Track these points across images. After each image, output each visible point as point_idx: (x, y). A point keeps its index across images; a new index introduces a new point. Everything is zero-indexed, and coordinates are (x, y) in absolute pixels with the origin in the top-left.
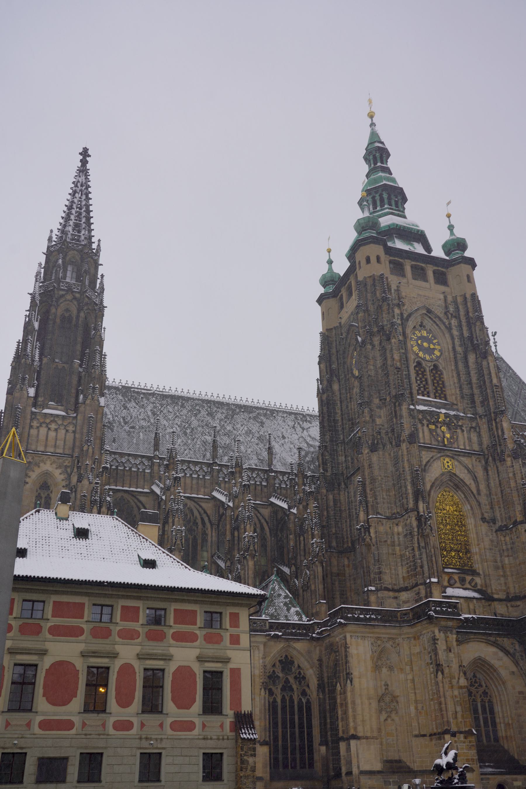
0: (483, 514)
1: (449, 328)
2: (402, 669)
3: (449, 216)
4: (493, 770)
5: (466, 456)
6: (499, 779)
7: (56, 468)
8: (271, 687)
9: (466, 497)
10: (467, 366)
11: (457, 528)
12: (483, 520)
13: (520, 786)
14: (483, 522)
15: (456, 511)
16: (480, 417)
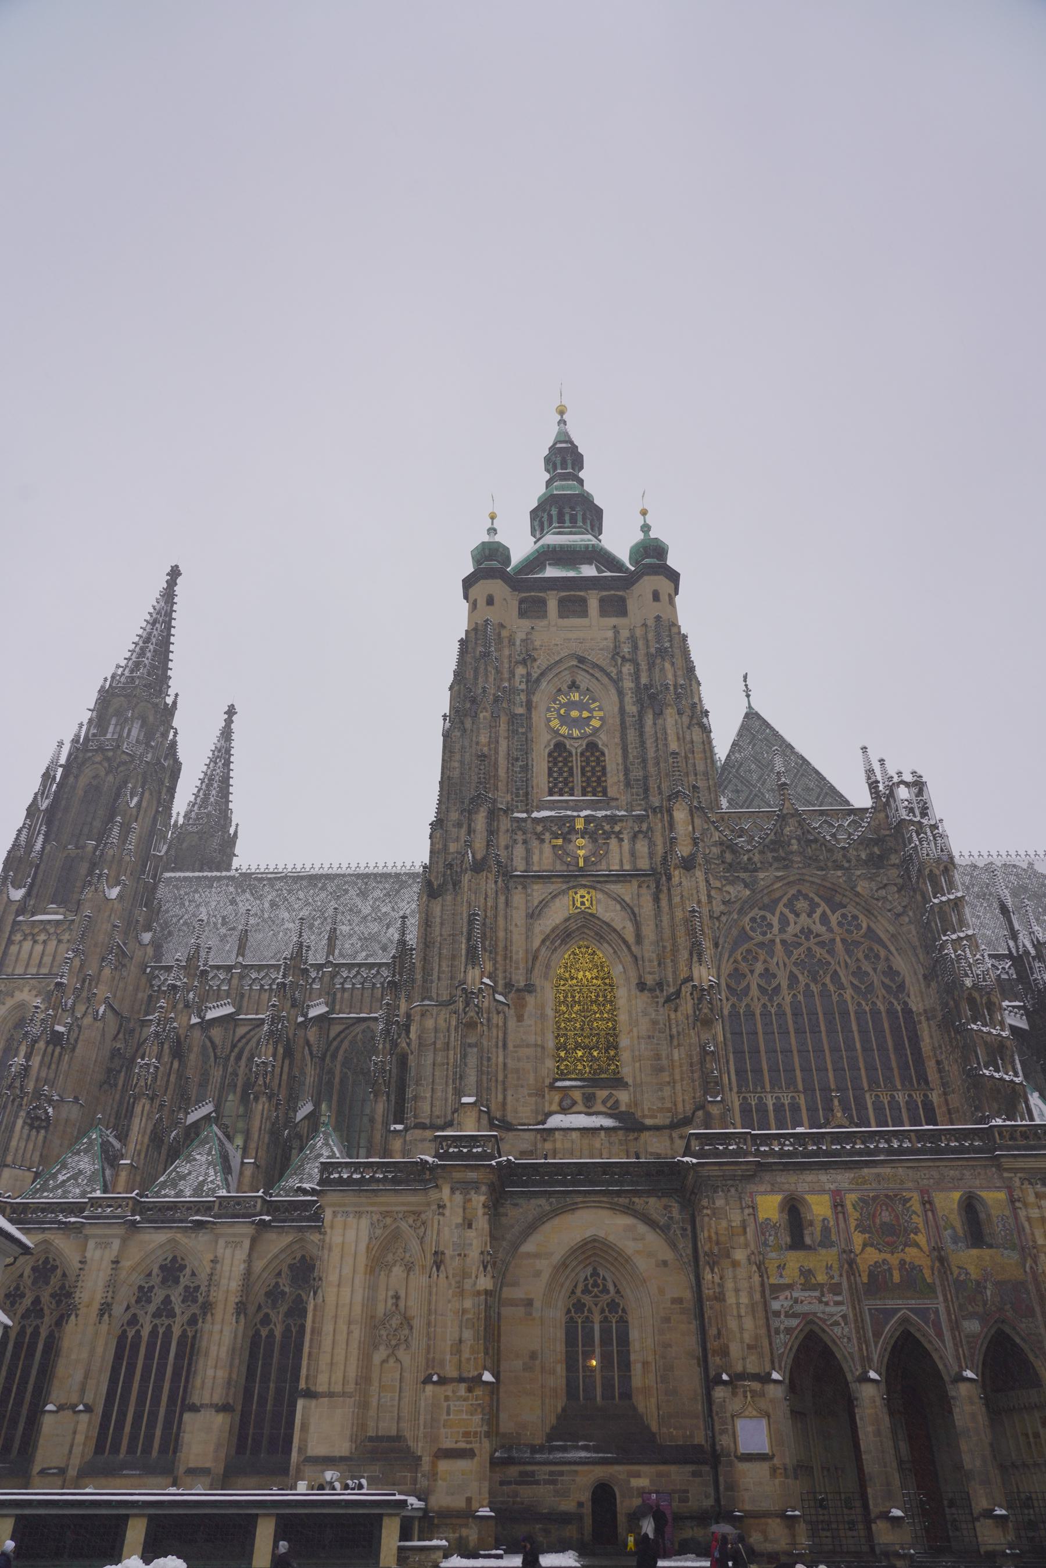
0: (640, 977)
1: (617, 682)
2: (423, 1267)
3: (644, 513)
4: (589, 1455)
5: (620, 882)
6: (600, 1472)
7: (36, 996)
8: (266, 1310)
9: (615, 952)
10: (641, 734)
11: (594, 1007)
12: (642, 986)
13: (643, 1488)
14: (642, 990)
15: (596, 978)
16: (654, 810)
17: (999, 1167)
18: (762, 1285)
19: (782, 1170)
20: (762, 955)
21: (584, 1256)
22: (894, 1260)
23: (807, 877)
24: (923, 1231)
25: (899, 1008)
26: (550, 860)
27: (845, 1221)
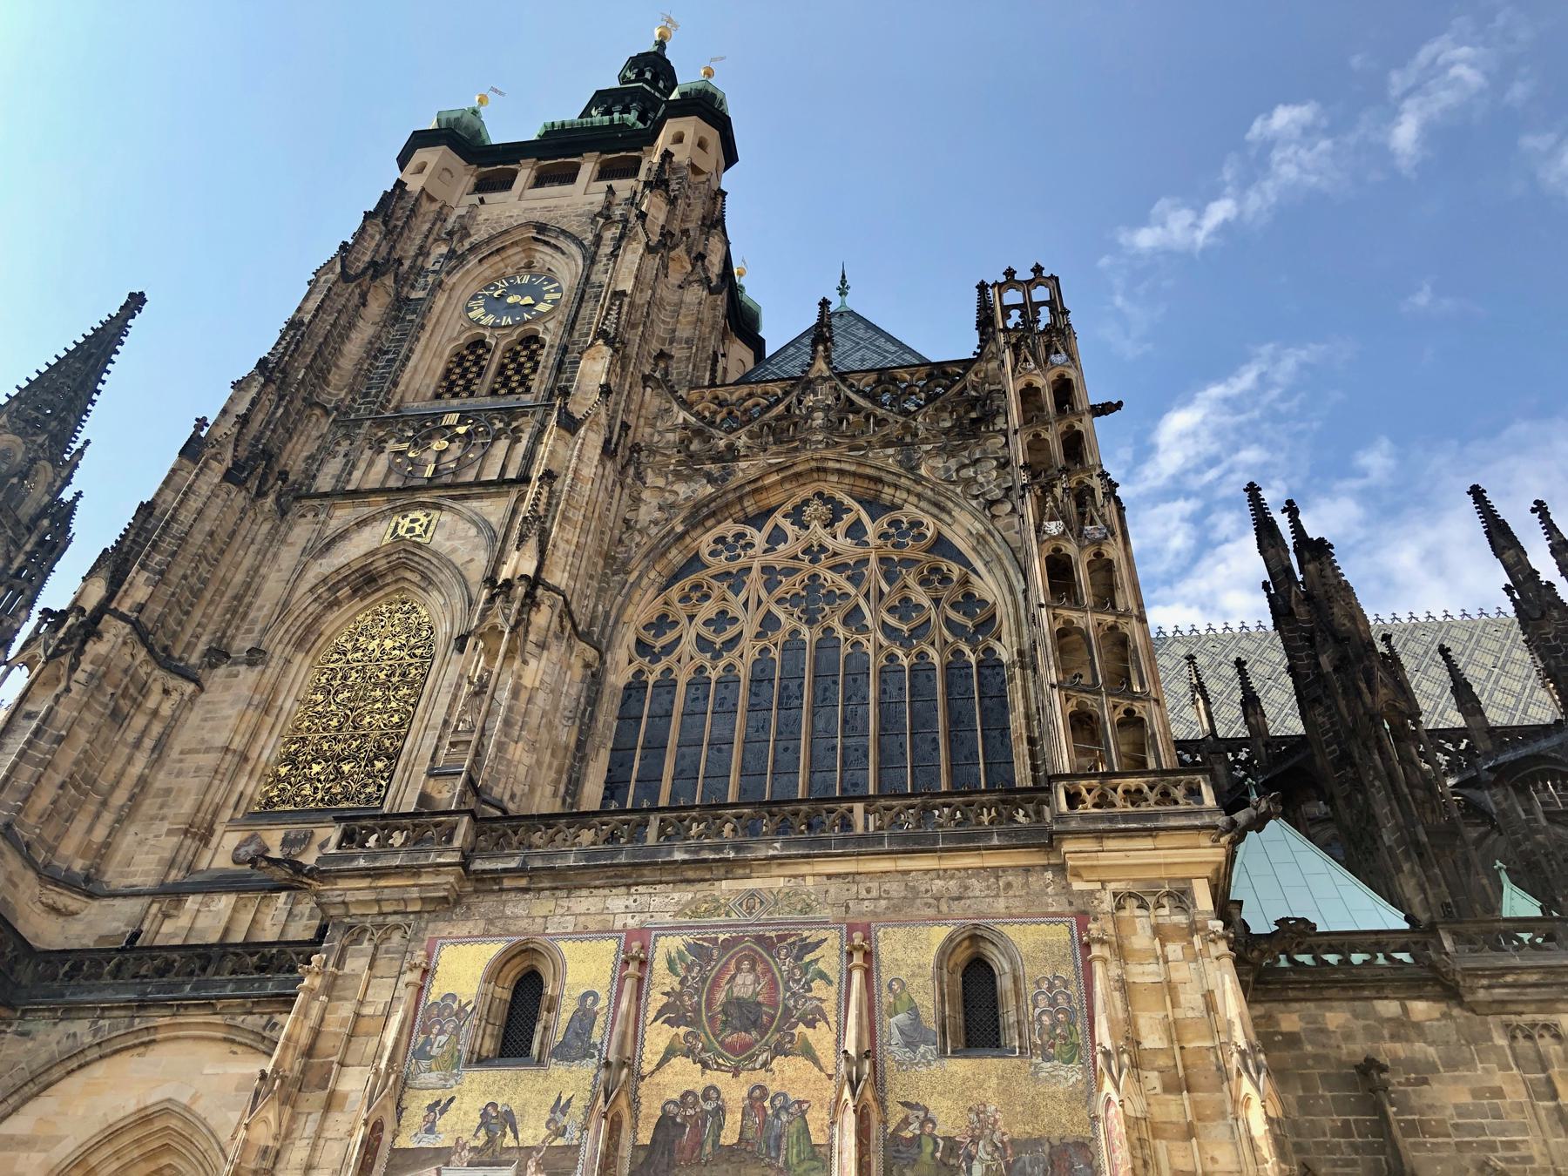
5: (490, 496)
11: (378, 693)
15: (400, 649)
17: (1061, 869)
18: (370, 1147)
19: (525, 890)
20: (719, 588)
21: (136, 1154)
22: (734, 1091)
23: (831, 464)
24: (832, 1019)
25: (973, 659)
26: (381, 476)
27: (638, 998)
